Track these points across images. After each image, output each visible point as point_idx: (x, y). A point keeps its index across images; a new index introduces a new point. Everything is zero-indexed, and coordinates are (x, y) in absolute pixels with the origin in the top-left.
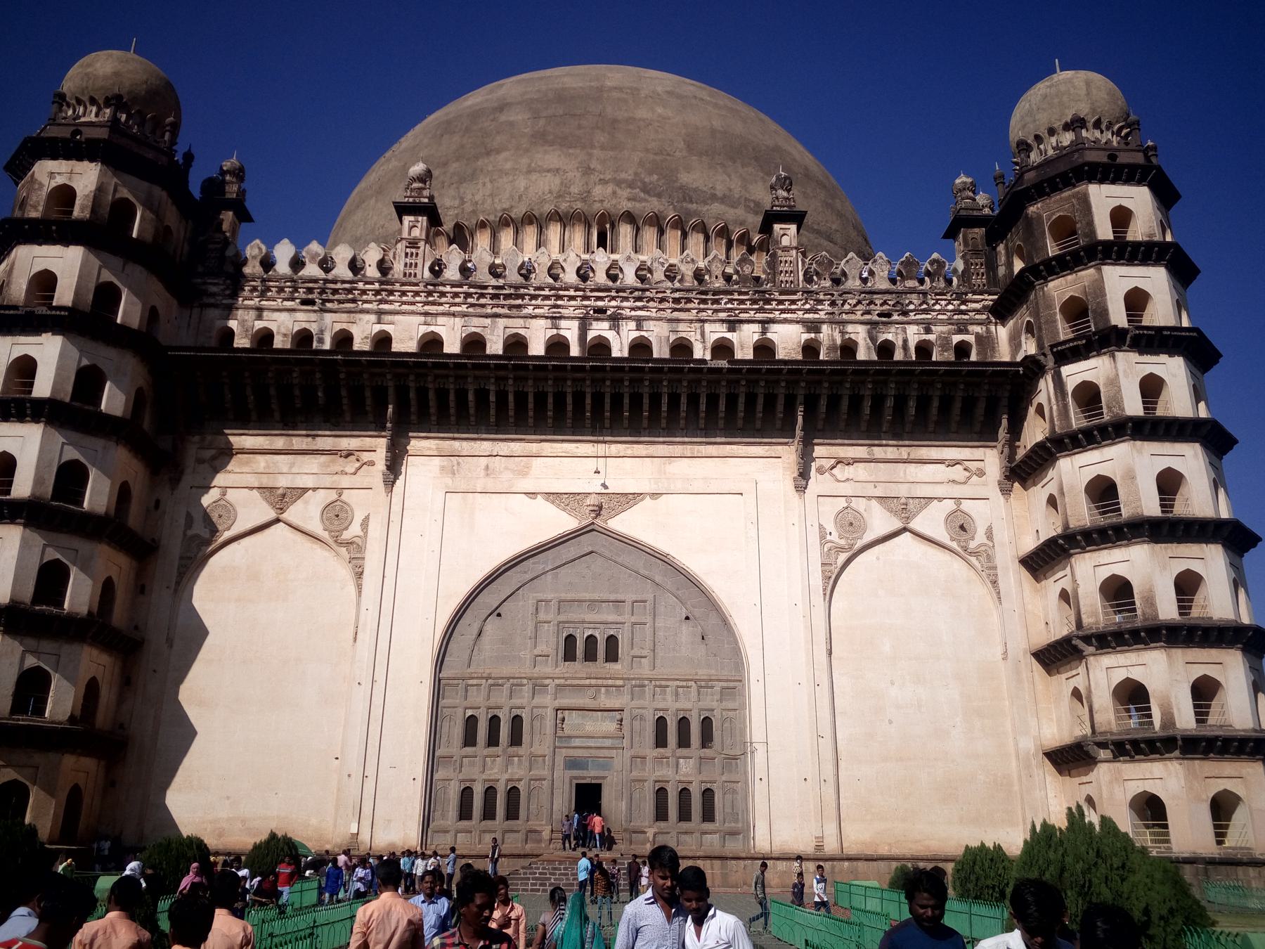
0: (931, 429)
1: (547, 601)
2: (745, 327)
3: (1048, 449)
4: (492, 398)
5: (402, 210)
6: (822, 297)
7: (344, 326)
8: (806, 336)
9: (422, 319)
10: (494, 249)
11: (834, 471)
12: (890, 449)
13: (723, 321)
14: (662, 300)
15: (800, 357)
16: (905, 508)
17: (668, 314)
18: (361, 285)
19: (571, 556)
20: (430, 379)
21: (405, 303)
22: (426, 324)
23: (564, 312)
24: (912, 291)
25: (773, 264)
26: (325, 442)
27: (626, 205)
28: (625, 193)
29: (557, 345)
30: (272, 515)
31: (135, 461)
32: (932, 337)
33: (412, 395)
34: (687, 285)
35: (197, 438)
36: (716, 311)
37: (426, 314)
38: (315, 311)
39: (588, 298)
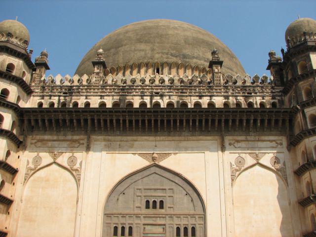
0: (265, 130)
1: (139, 189)
2: (205, 98)
3: (301, 136)
4: (121, 122)
5: (95, 64)
7: (76, 100)
8: (224, 100)
10: (124, 75)
11: (236, 145)
13: (197, 96)
15: (223, 107)
16: (257, 157)
17: (180, 94)
18: (81, 87)
20: (101, 116)
21: (94, 92)
22: (101, 99)
23: (146, 94)
24: (258, 86)
25: (213, 77)
26: (69, 137)
27: (165, 60)
28: (165, 56)
30: (52, 161)
31: (12, 144)
33: (96, 121)
35: (31, 137)
39: (153, 89)
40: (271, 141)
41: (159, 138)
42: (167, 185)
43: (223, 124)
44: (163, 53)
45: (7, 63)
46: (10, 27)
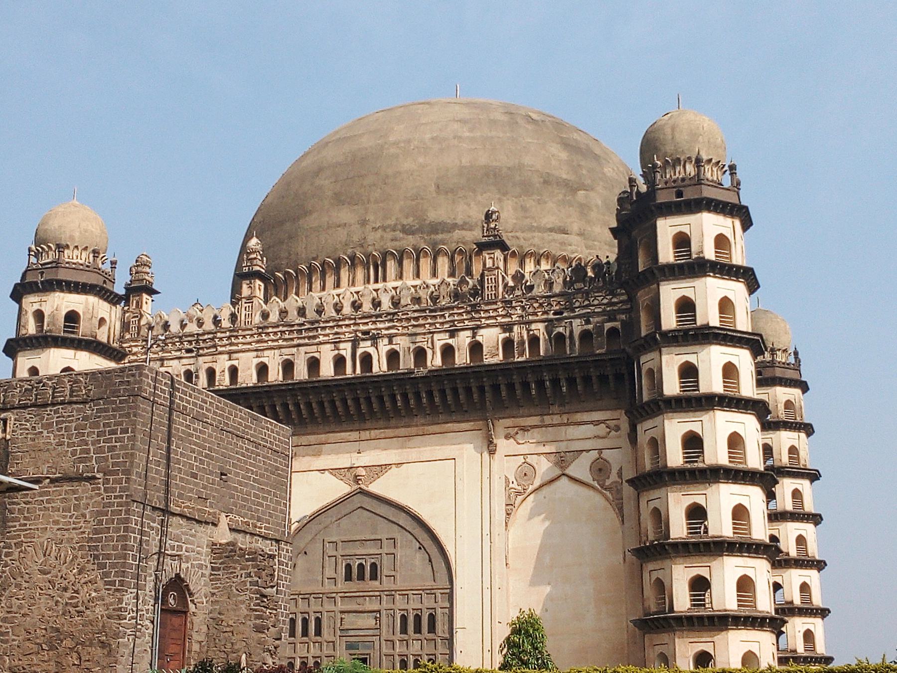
2: (462, 333)
6: (514, 304)
7: (210, 365)
9: (255, 353)
11: (518, 436)
12: (556, 416)
13: (446, 331)
14: (408, 320)
17: (412, 330)
18: (219, 335)
19: (347, 511)
21: (244, 344)
22: (257, 357)
28: (389, 235)
29: (339, 362)
32: (590, 327)
34: (424, 305)
36: (442, 324)
37: (256, 350)
38: (193, 357)
39: (358, 324)
40: (596, 423)
41: (368, 432)
42: (384, 531)
43: (488, 396)
44: (384, 228)
45: (64, 313)
46: (60, 227)
